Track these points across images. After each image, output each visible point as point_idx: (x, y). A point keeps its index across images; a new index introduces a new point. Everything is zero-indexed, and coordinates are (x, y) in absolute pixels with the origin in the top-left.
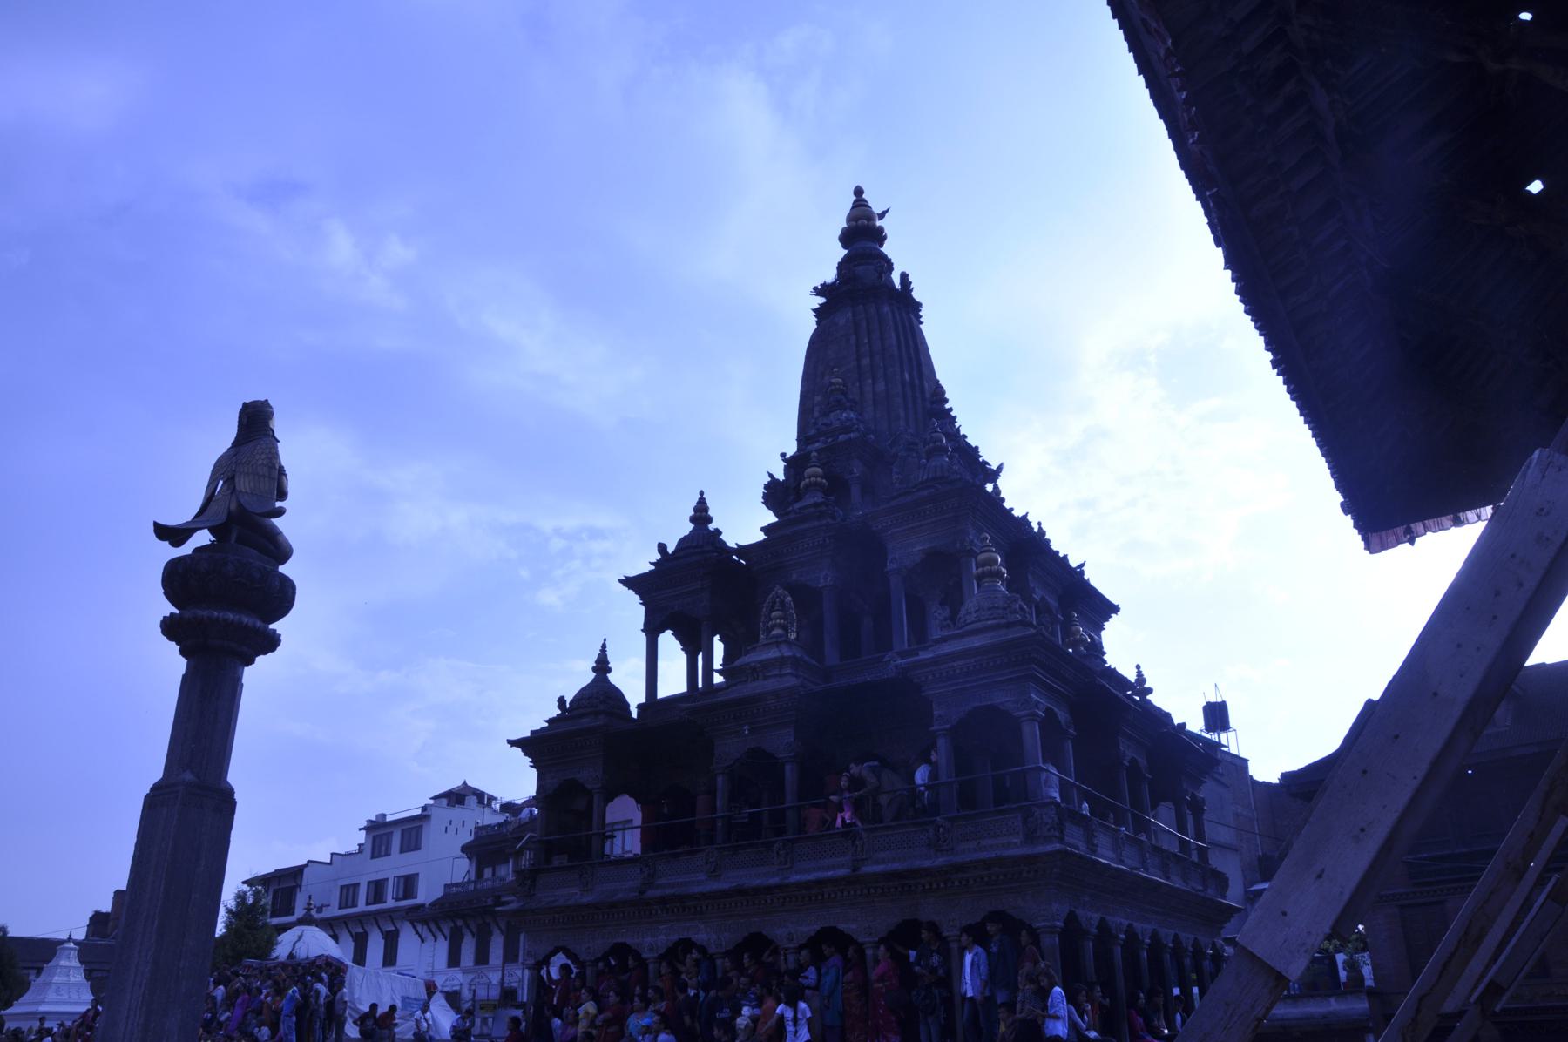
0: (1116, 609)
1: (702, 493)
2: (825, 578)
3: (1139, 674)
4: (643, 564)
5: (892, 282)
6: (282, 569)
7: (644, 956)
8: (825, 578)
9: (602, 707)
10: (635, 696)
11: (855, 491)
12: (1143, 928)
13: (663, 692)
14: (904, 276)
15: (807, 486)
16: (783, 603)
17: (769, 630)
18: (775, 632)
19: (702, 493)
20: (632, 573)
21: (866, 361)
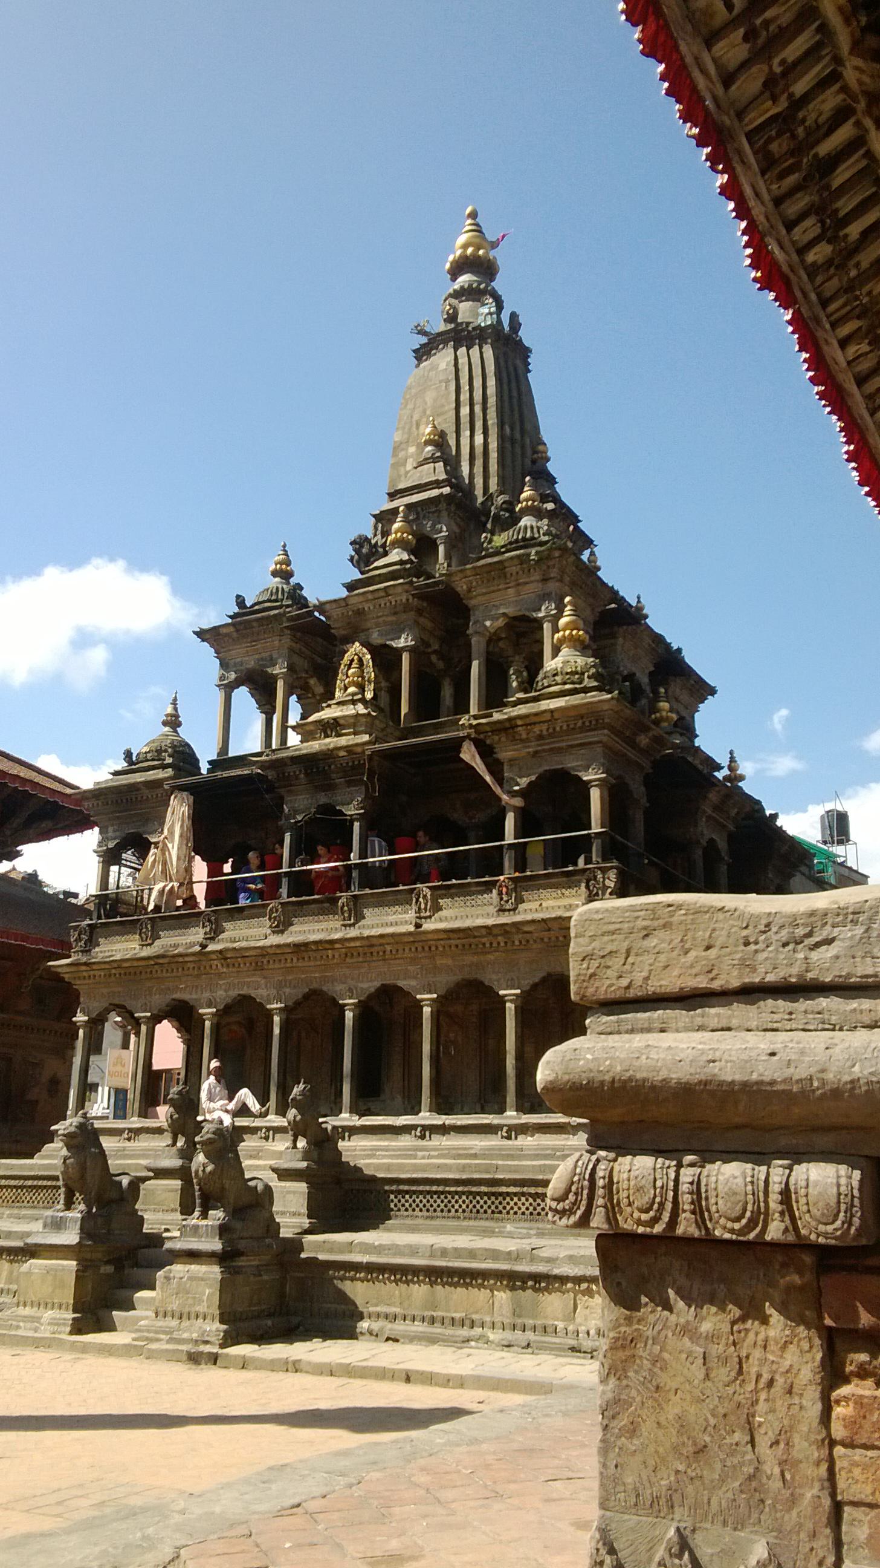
0: (712, 691)
10: (206, 754)
13: (235, 750)
14: (514, 316)
16: (360, 660)
17: (346, 689)
18: (352, 689)
20: (206, 626)
21: (465, 411)
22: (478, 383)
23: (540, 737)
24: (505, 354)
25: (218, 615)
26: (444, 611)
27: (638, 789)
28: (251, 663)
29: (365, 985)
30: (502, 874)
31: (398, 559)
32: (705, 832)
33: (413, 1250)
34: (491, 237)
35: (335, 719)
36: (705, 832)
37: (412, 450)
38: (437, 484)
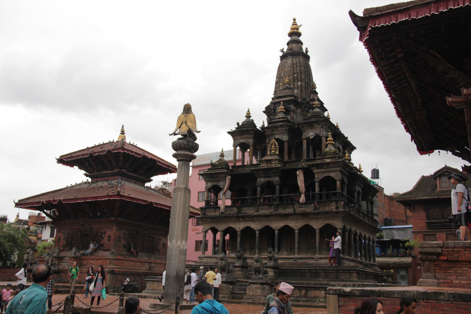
0: (355, 148)
3: (360, 166)
9: (225, 167)
12: (358, 231)
14: (306, 49)
15: (280, 112)
16: (275, 144)
17: (271, 151)
18: (273, 151)
21: (295, 75)
25: (233, 128)
26: (295, 132)
27: (346, 180)
29: (280, 225)
30: (315, 200)
31: (281, 117)
33: (302, 284)
34: (299, 24)
35: (270, 160)
37: (281, 84)
38: (290, 96)
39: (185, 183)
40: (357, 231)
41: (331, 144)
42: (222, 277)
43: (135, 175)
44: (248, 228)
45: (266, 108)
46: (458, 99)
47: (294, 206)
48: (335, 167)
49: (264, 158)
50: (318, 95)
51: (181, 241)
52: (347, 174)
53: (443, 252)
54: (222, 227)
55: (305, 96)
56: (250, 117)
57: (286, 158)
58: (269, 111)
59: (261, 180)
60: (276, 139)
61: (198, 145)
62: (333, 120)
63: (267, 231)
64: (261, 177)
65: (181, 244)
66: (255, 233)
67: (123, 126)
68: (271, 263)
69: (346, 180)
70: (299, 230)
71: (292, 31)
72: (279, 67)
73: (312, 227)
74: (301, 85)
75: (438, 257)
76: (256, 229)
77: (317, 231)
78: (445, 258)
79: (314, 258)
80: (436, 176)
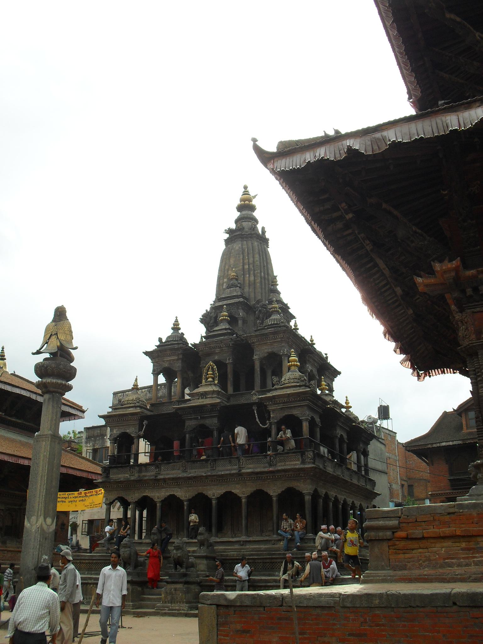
0: (339, 373)
1: (176, 318)
2: (229, 360)
4: (152, 346)
5: (258, 230)
6: (71, 364)
7: (155, 500)
8: (229, 360)
9: (138, 404)
11: (240, 322)
12: (341, 498)
14: (263, 229)
15: (222, 320)
16: (212, 368)
18: (210, 379)
19: (176, 318)
21: (246, 267)
22: (251, 256)
23: (284, 403)
24: (261, 243)
27: (318, 420)
28: (166, 365)
29: (220, 492)
31: (224, 327)
32: (339, 432)
34: (252, 194)
35: (205, 392)
36: (339, 432)
37: (225, 280)
38: (237, 297)
39: (53, 427)
40: (339, 497)
41: (294, 365)
42: (128, 574)
43: (20, 421)
44: (172, 497)
45: (202, 316)
46: (432, 280)
47: (239, 461)
48: (299, 401)
49: (196, 391)
50: (281, 296)
51: (45, 519)
52: (320, 411)
53: (401, 525)
54: (134, 497)
55: (260, 298)
56: (180, 329)
57: (230, 390)
58: (209, 320)
59: (190, 424)
60: (215, 362)
61: (75, 370)
62: (305, 332)
63: (200, 503)
64: (191, 419)
65: (44, 523)
66: (183, 505)
67: (3, 348)
68: (203, 552)
69: (318, 420)
70: (248, 497)
71: (243, 202)
72: (224, 254)
73: (267, 493)
74: (255, 280)
75: (393, 533)
76: (183, 498)
77: (274, 499)
78: (402, 534)
79: (270, 541)
80: (460, 411)
